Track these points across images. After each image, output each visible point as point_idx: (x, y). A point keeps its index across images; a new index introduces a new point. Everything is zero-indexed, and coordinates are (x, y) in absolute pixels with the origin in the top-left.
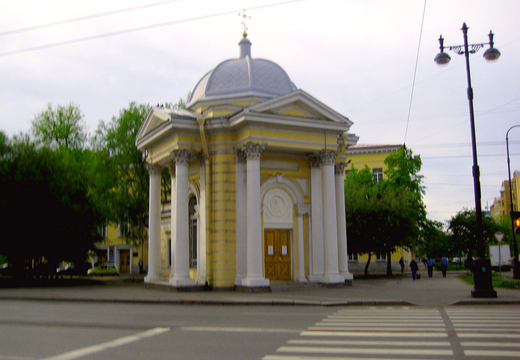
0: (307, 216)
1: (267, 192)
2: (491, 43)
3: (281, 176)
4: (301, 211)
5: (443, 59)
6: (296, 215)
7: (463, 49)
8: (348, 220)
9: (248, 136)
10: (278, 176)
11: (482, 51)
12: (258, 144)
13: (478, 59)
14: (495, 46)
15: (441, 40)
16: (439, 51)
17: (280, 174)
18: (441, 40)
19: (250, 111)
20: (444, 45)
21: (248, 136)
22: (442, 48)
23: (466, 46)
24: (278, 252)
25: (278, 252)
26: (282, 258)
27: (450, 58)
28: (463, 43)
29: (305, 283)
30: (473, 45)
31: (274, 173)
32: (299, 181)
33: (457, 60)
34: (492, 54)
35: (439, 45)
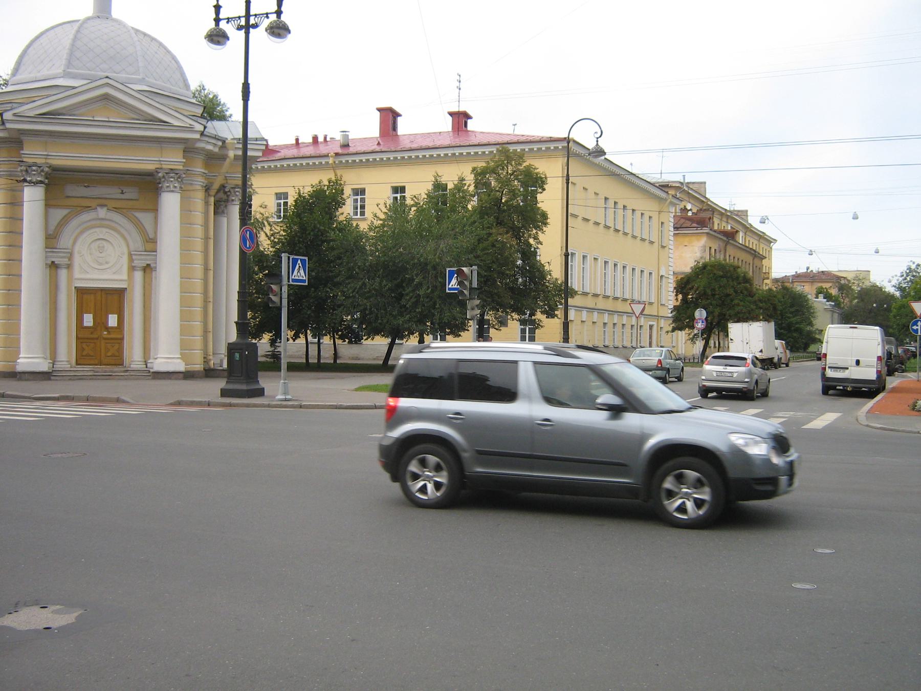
0: (148, 269)
1: (82, 233)
2: (279, 13)
3: (105, 209)
4: (140, 262)
5: (217, 37)
6: (132, 269)
7: (243, 22)
8: (19, 305)
9: (33, 153)
10: (99, 209)
11: (266, 23)
12: (35, 164)
13: (259, 35)
14: (283, 17)
15: (218, 8)
16: (212, 25)
17: (102, 206)
18: (218, 8)
19: (15, 115)
20: (221, 16)
21: (33, 153)
22: (217, 20)
23: (248, 15)
24: (101, 323)
25: (101, 323)
26: (109, 332)
27: (228, 39)
28: (243, 13)
29: (342, 338)
30: (256, 15)
31: (93, 203)
32: (140, 215)
33: (236, 37)
34: (279, 30)
35: (214, 16)
